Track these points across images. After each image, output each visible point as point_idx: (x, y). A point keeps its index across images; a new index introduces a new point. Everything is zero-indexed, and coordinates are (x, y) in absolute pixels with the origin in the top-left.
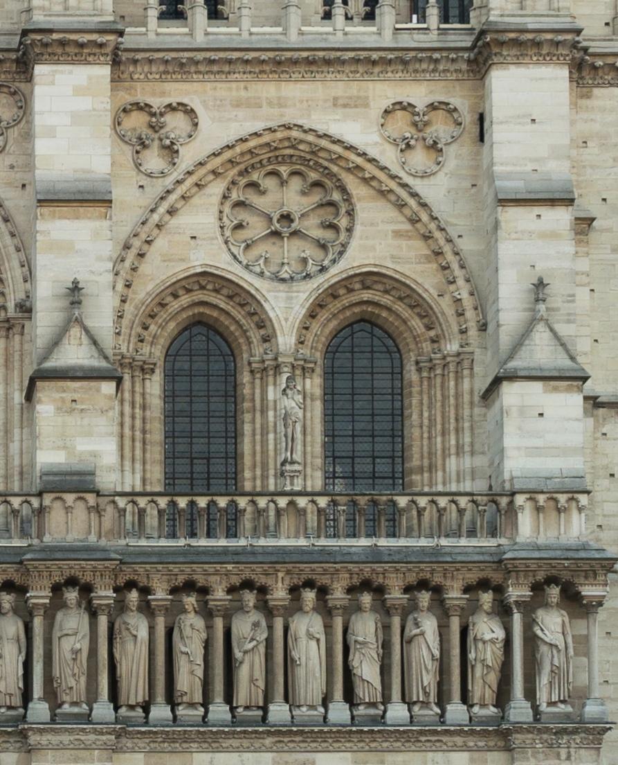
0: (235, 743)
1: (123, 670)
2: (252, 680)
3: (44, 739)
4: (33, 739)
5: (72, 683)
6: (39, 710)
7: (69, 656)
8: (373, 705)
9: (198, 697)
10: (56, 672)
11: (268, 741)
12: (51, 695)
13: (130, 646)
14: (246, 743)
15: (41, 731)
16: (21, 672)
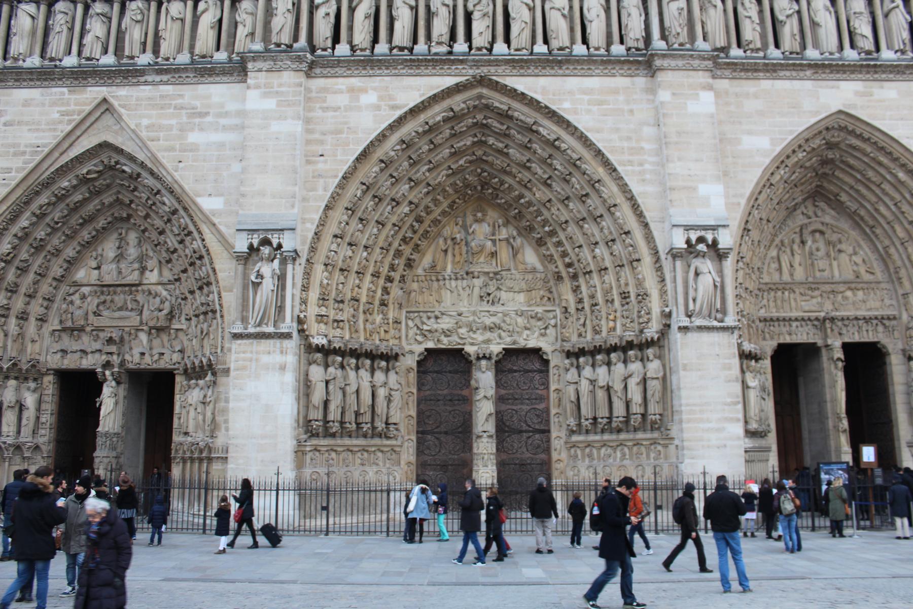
0: (788, 73)
1: (709, 28)
2: (793, 35)
3: (665, 63)
4: (658, 62)
5: (679, 30)
6: (658, 44)
7: (676, 13)
8: (868, 53)
9: (759, 45)
10: (667, 24)
11: (809, 73)
12: (664, 37)
13: (712, 11)
14: (794, 74)
15: (664, 56)
16: (643, 27)
